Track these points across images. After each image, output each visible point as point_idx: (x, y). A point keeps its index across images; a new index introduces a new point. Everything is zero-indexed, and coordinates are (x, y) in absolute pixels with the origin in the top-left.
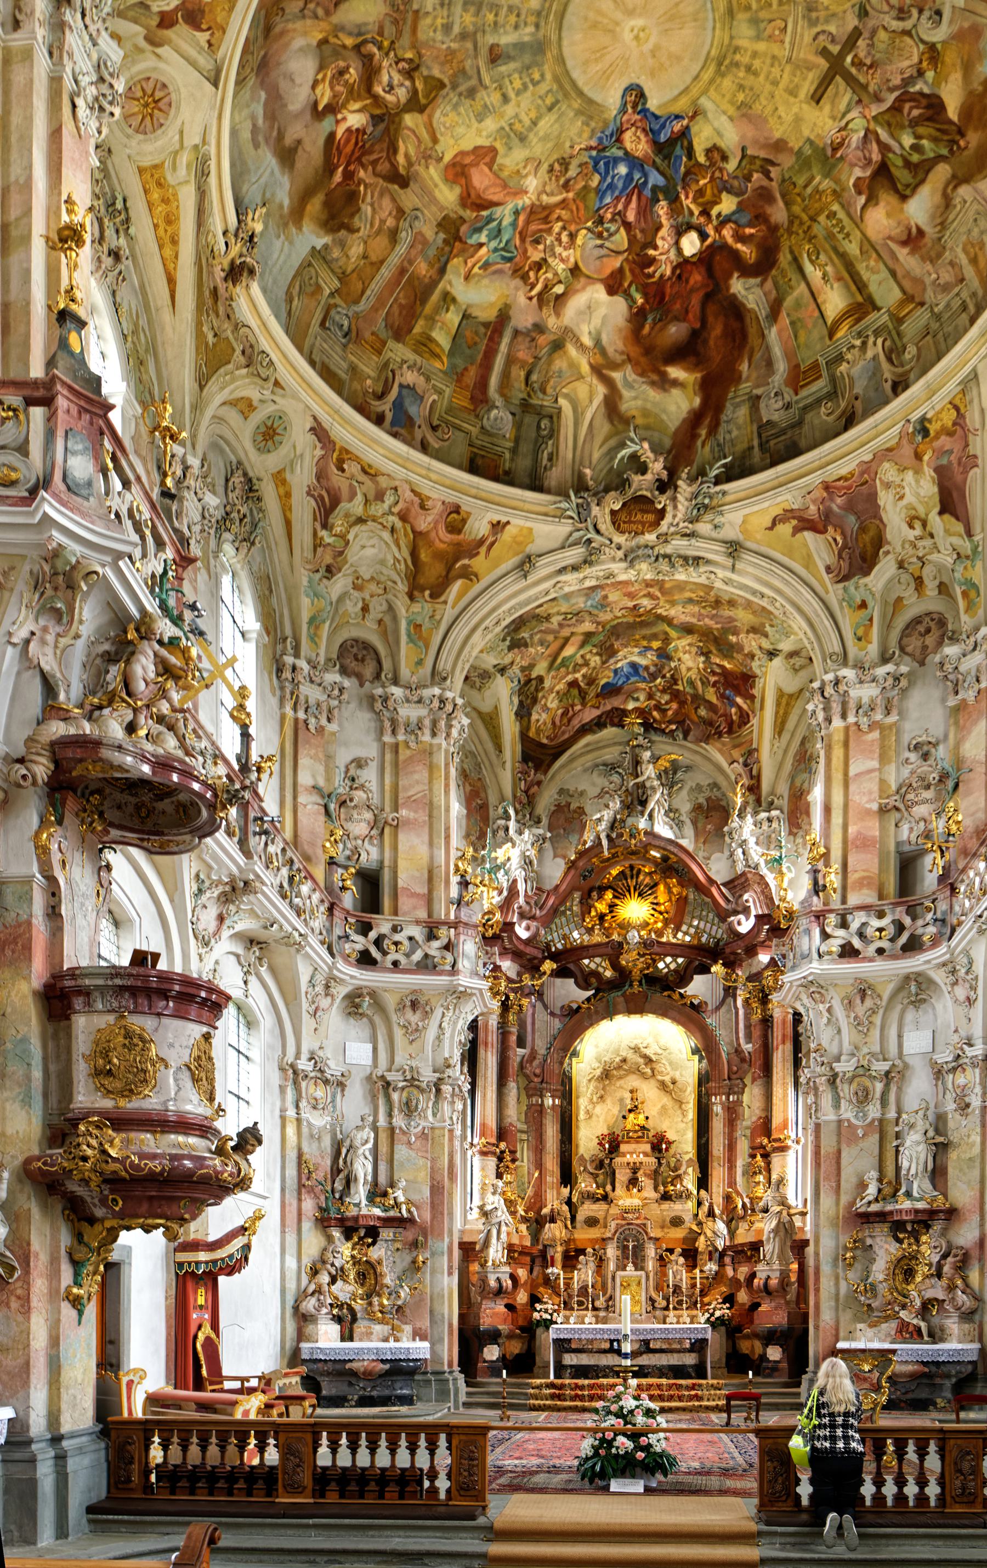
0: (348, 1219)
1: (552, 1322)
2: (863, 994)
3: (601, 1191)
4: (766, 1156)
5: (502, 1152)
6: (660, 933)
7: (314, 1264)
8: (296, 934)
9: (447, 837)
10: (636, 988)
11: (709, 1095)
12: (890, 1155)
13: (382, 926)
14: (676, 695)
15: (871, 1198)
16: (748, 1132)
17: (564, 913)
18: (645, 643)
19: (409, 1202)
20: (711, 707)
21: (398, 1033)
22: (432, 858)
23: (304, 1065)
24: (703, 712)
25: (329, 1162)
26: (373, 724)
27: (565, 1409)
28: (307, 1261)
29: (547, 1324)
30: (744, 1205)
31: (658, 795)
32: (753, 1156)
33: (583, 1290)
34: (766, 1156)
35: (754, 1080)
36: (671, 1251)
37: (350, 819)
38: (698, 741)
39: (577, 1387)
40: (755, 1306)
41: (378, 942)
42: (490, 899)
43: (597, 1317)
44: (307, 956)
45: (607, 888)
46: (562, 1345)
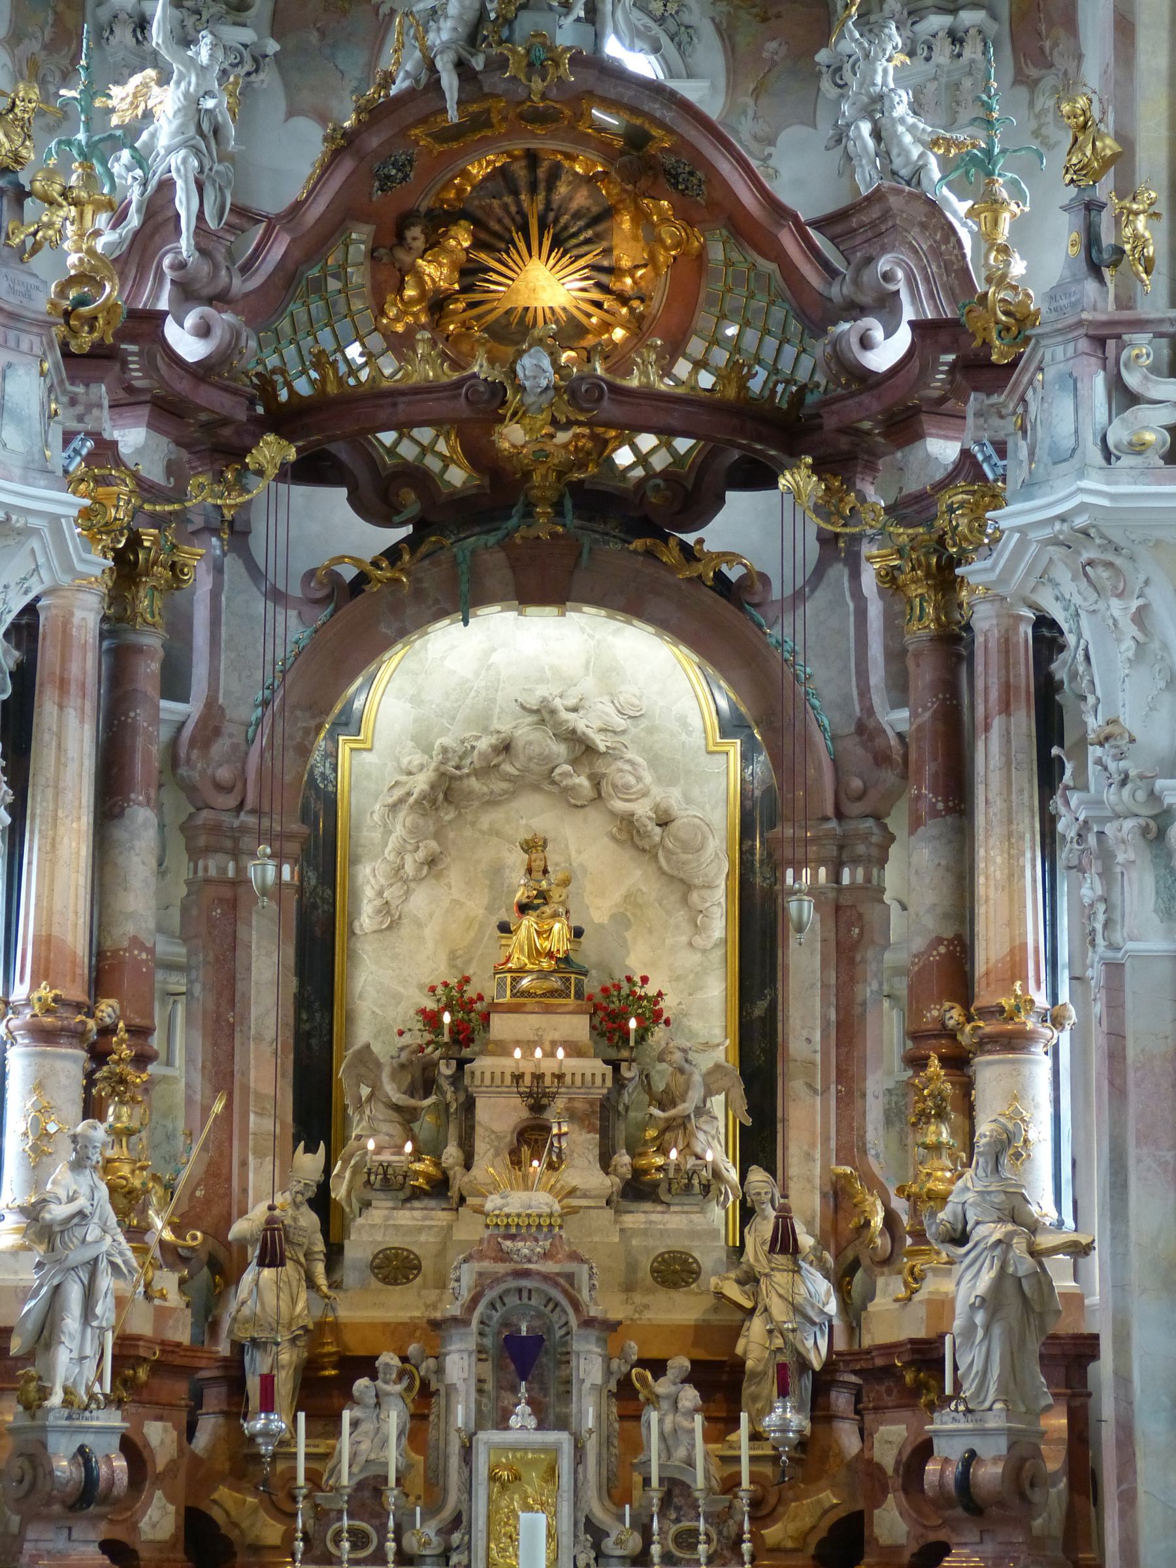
5: (106, 1031)
11: (775, 866)
16: (901, 986)
35: (915, 824)
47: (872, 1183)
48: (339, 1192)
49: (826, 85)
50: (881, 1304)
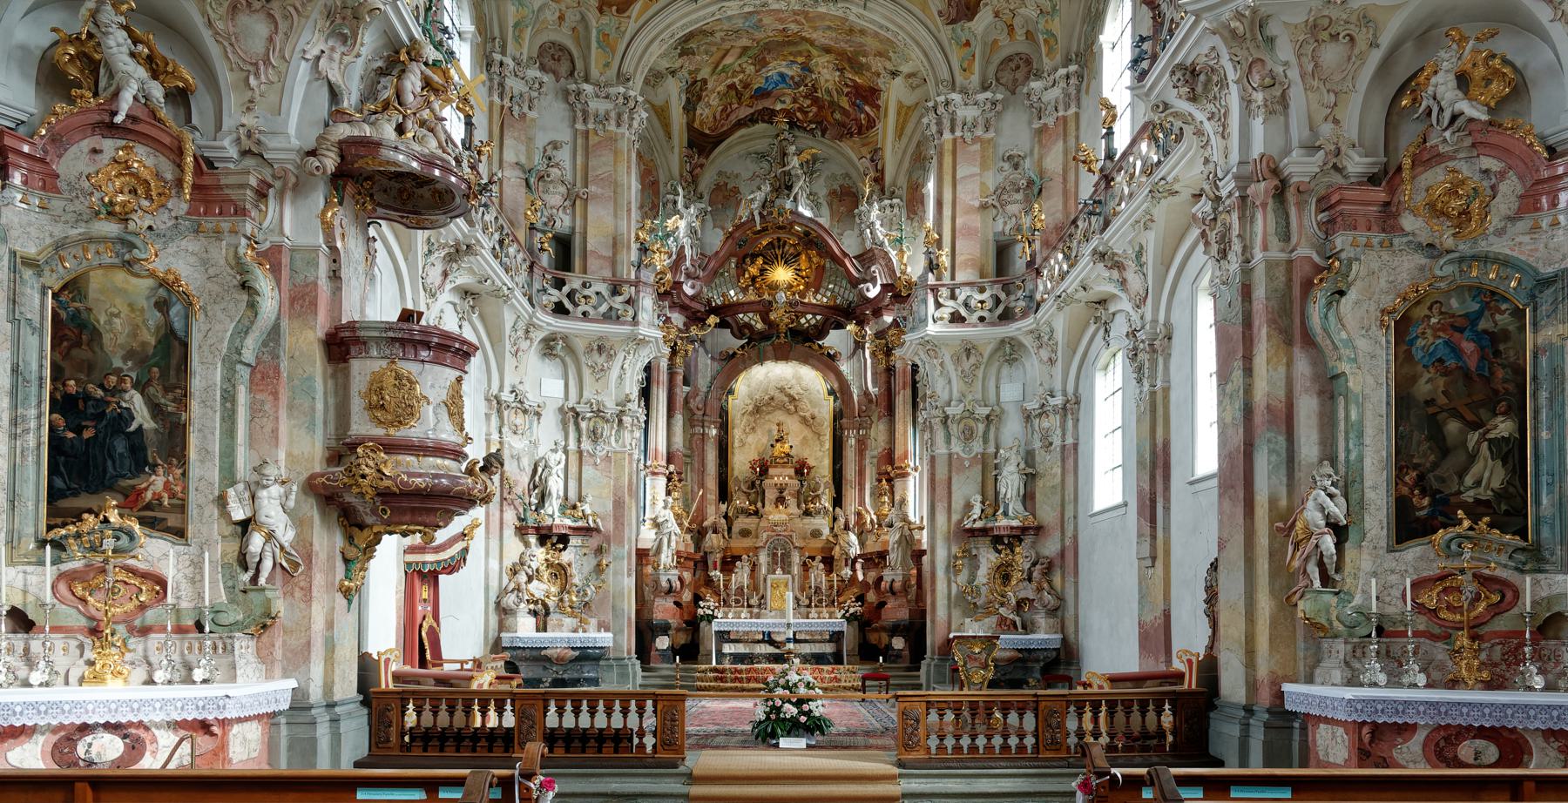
0: (543, 528)
1: (714, 617)
2: (968, 352)
3: (753, 507)
4: (889, 480)
5: (671, 473)
6: (802, 295)
7: (514, 565)
8: (505, 288)
9: (629, 210)
10: (782, 340)
11: (842, 429)
12: (990, 482)
13: (574, 282)
14: (815, 101)
15: (975, 517)
16: (875, 460)
17: (722, 274)
18: (792, 58)
19: (594, 514)
20: (844, 112)
21: (586, 372)
22: (616, 227)
23: (506, 396)
24: (838, 116)
26: (567, 114)
27: (726, 689)
28: (508, 563)
29: (710, 618)
30: (872, 521)
31: (801, 182)
32: (880, 481)
33: (740, 590)
34: (889, 480)
36: (813, 558)
37: (546, 192)
38: (834, 138)
39: (736, 671)
40: (882, 604)
41: (570, 296)
42: (661, 261)
43: (751, 613)
44: (513, 306)
45: (758, 256)
46: (723, 637)
47: (867, 511)
48: (730, 514)
49: (858, 221)
50: (869, 542)
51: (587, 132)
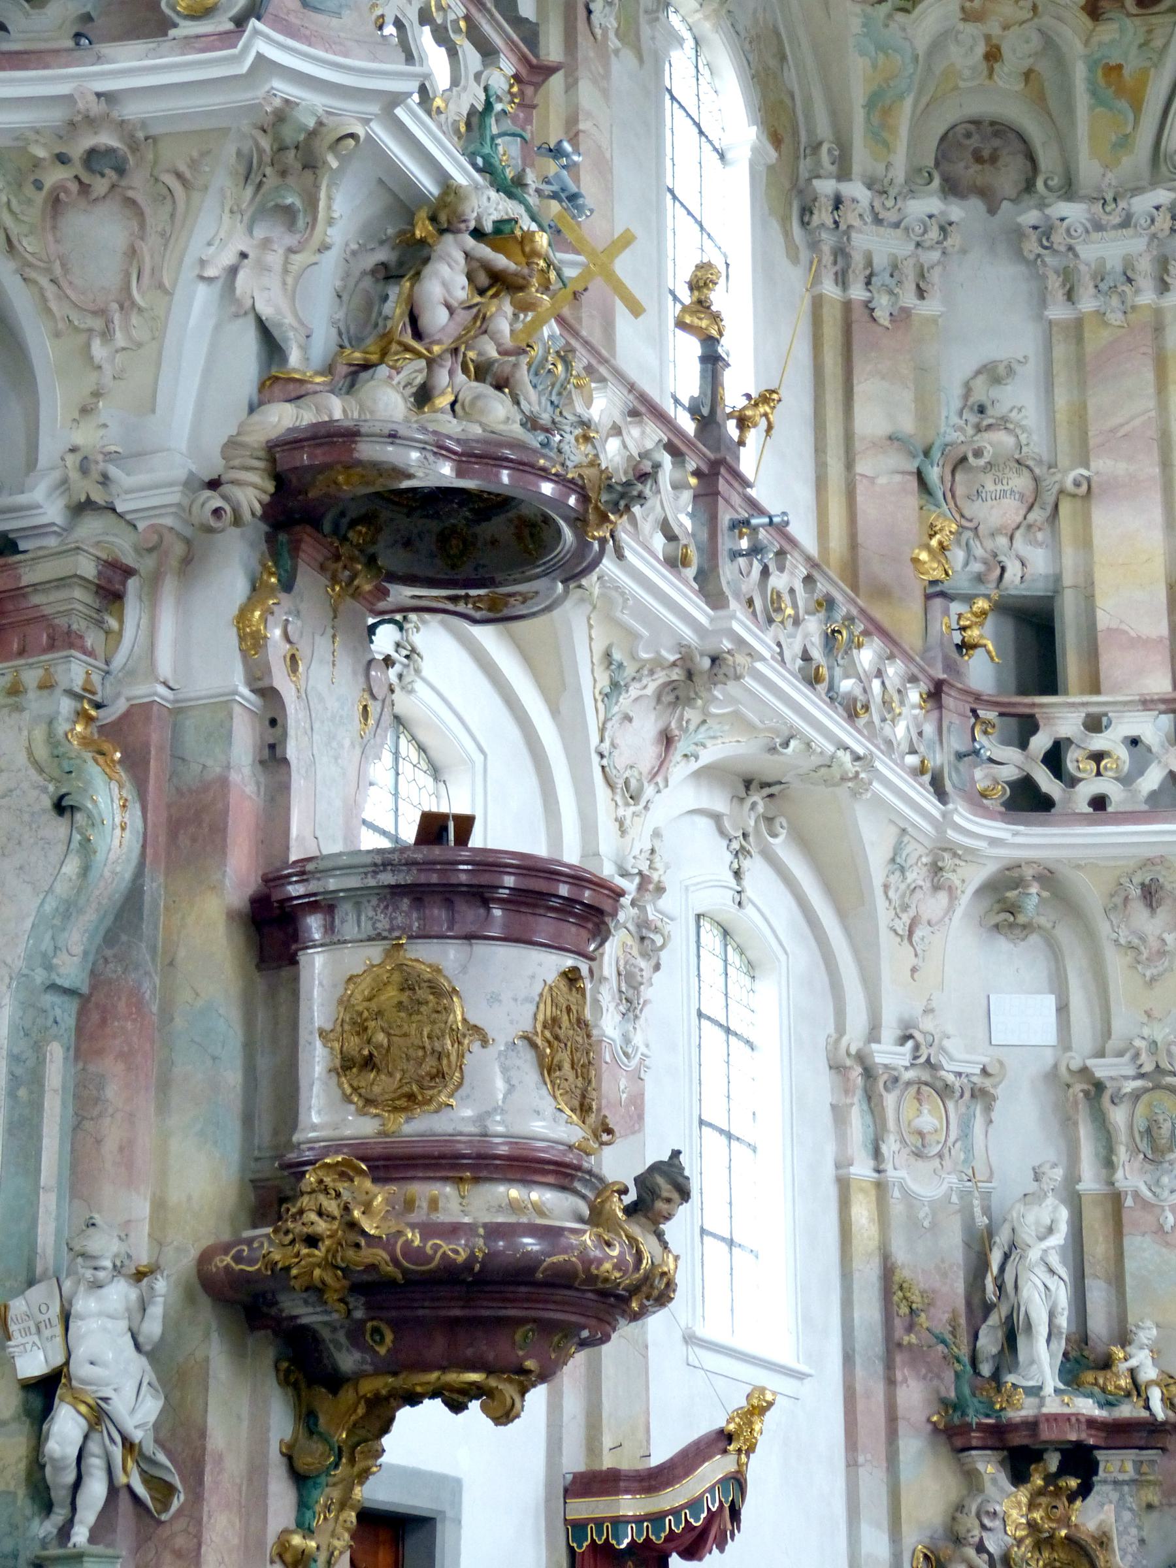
0: (1012, 1427)
21: (1116, 964)
25: (960, 1287)
51: (1077, 328)
